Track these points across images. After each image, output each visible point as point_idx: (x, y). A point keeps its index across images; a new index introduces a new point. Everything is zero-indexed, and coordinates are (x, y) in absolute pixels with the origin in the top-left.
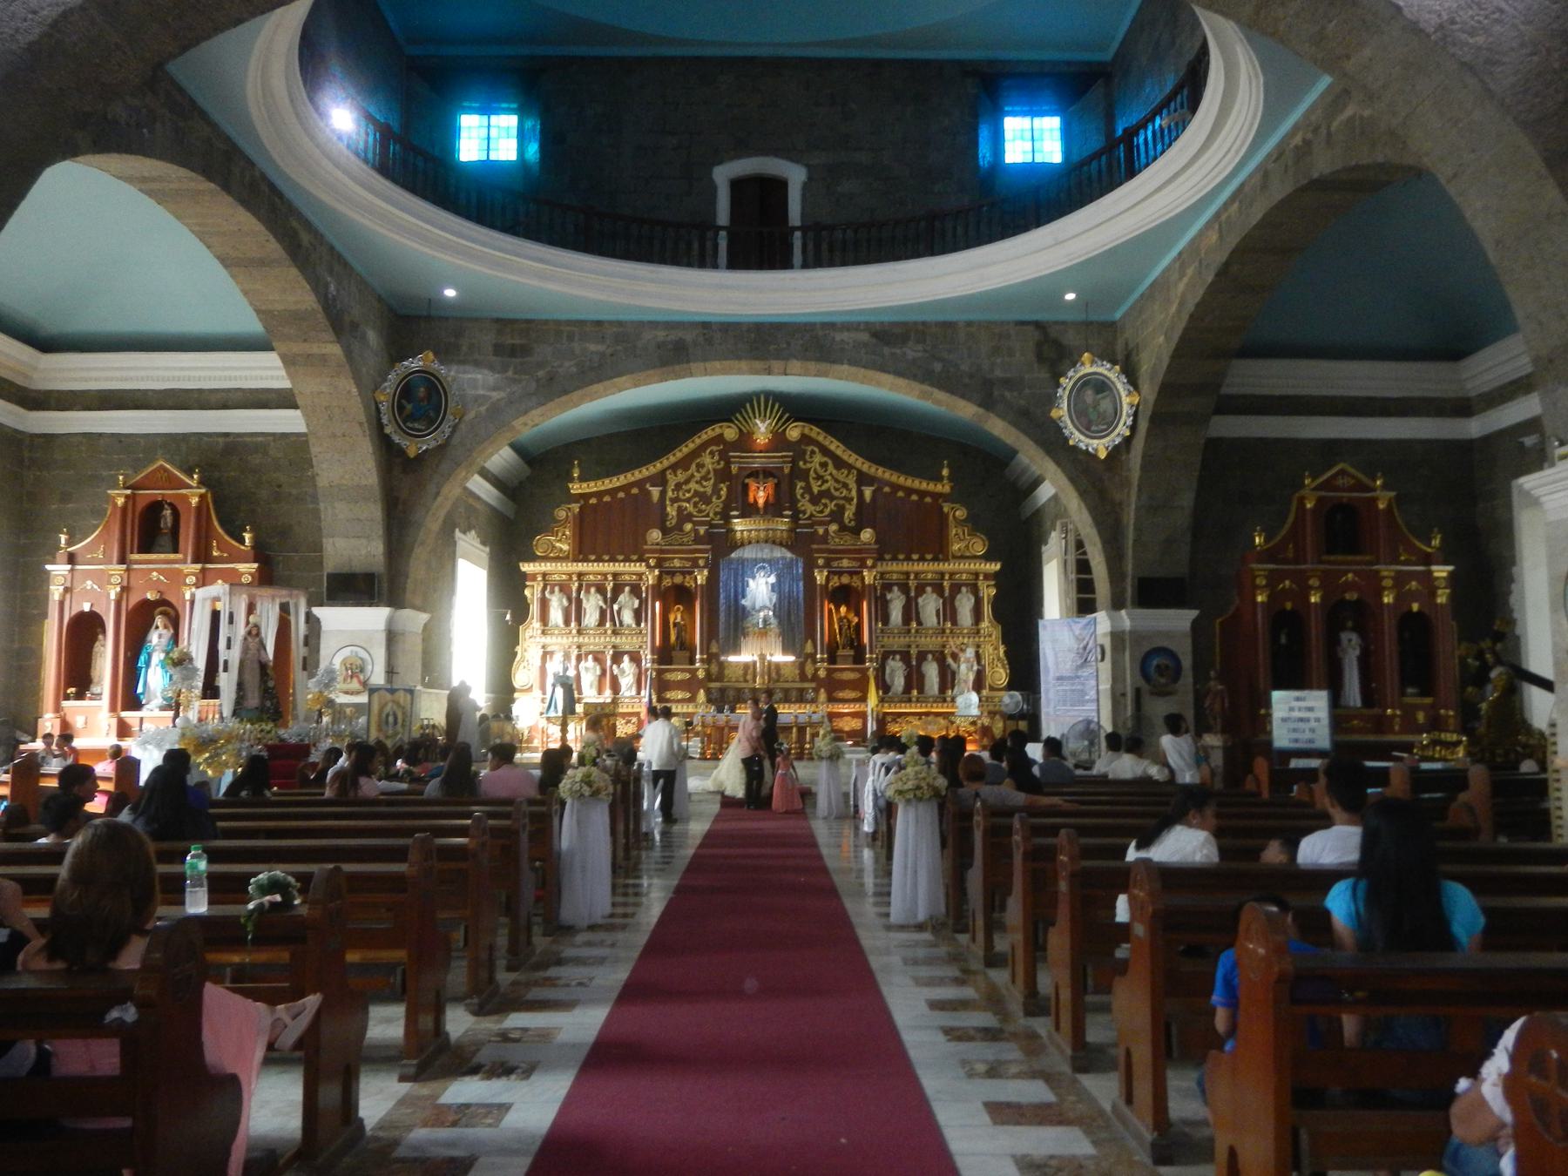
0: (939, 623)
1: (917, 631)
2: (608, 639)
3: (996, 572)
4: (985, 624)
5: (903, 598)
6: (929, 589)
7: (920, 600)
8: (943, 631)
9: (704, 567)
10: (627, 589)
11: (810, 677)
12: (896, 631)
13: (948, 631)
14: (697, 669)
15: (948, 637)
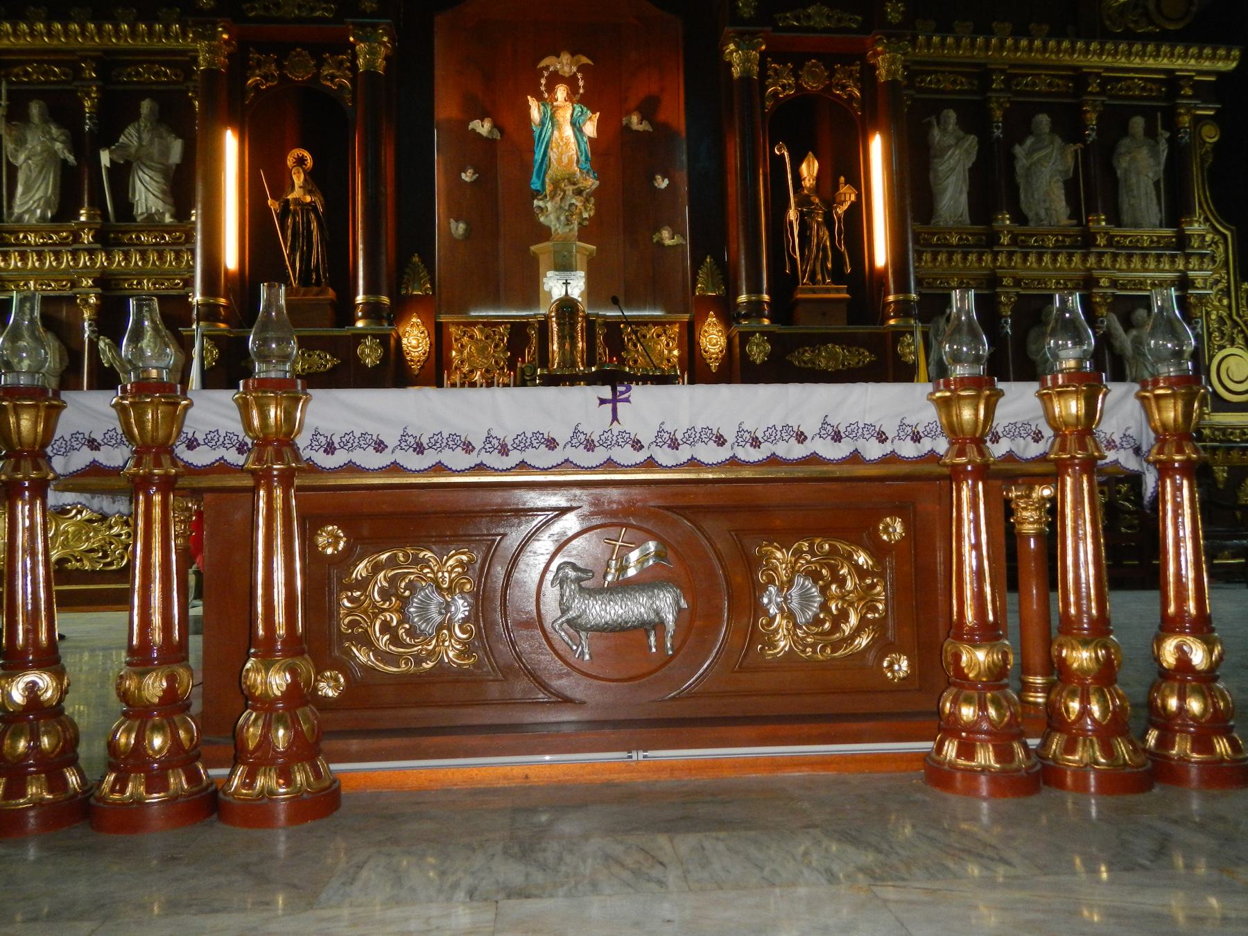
0: (1075, 214)
1: (1014, 240)
2: (84, 259)
3: (1219, 74)
4: (1196, 228)
5: (972, 140)
6: (1043, 120)
7: (1018, 150)
8: (1086, 241)
9: (373, 15)
10: (146, 106)
11: (714, 366)
12: (954, 240)
13: (1101, 241)
14: (359, 337)
15: (1100, 255)
